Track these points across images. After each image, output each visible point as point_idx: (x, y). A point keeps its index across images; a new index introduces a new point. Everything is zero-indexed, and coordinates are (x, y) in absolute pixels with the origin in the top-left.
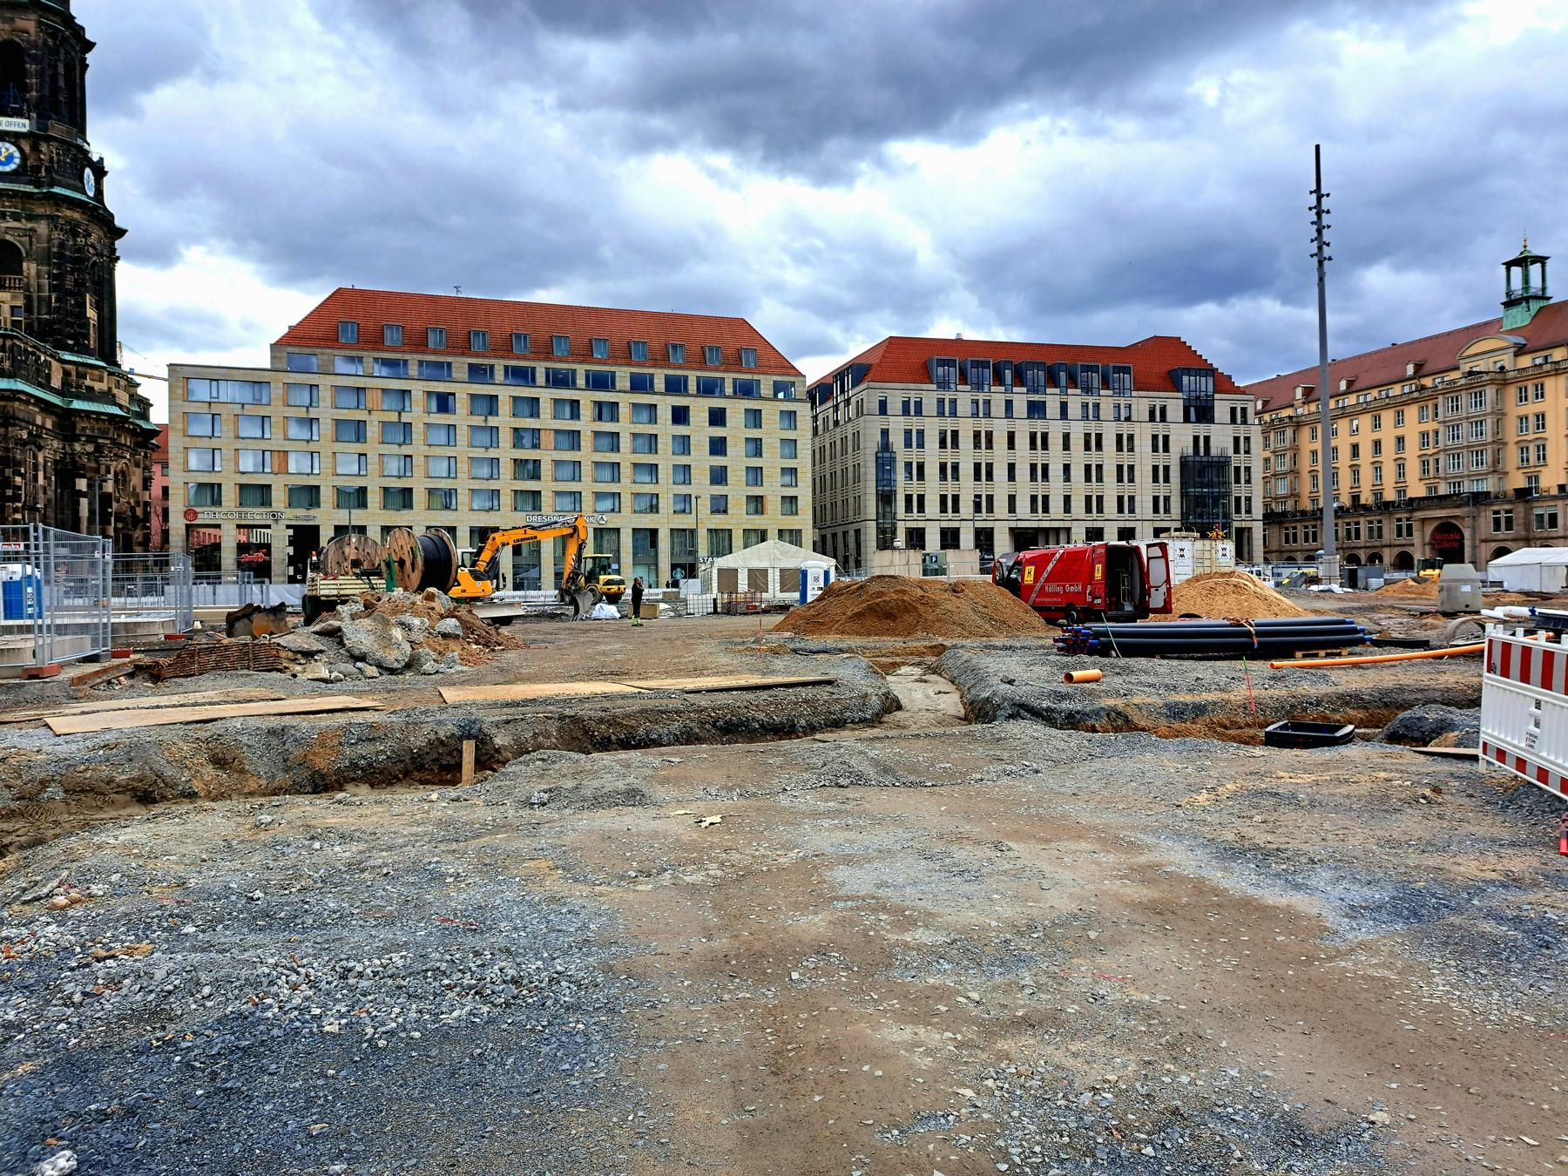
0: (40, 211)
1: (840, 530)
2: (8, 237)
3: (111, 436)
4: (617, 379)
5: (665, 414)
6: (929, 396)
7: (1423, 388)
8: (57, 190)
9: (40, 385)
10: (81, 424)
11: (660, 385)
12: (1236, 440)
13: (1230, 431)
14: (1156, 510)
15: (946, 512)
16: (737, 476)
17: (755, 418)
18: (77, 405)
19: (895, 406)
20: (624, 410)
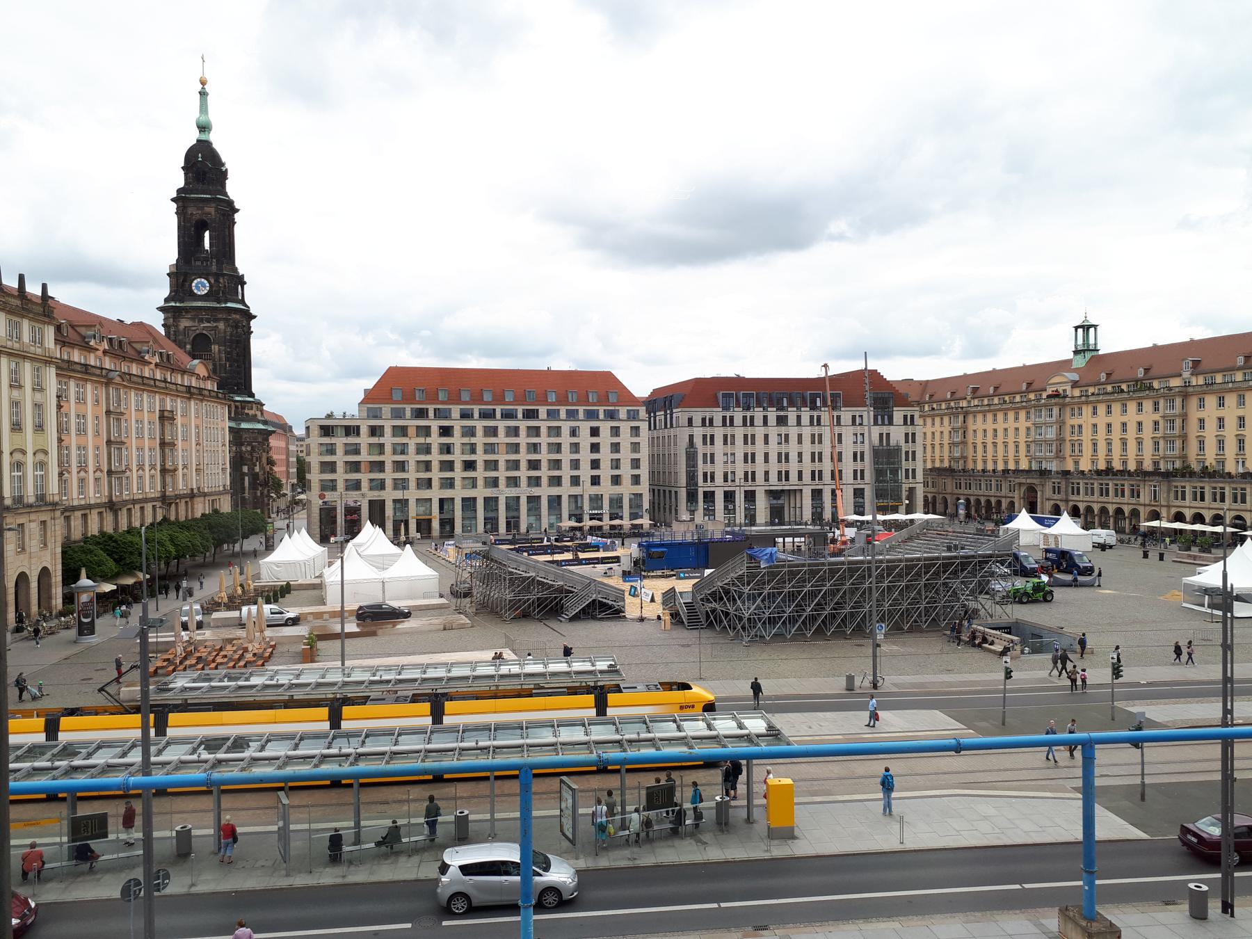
0: (220, 316)
1: (673, 490)
2: (204, 332)
4: (540, 413)
5: (565, 431)
6: (718, 414)
8: (229, 305)
11: (563, 415)
12: (907, 435)
13: (903, 430)
14: (855, 478)
17: (615, 431)
18: (244, 425)
19: (697, 420)
20: (544, 431)
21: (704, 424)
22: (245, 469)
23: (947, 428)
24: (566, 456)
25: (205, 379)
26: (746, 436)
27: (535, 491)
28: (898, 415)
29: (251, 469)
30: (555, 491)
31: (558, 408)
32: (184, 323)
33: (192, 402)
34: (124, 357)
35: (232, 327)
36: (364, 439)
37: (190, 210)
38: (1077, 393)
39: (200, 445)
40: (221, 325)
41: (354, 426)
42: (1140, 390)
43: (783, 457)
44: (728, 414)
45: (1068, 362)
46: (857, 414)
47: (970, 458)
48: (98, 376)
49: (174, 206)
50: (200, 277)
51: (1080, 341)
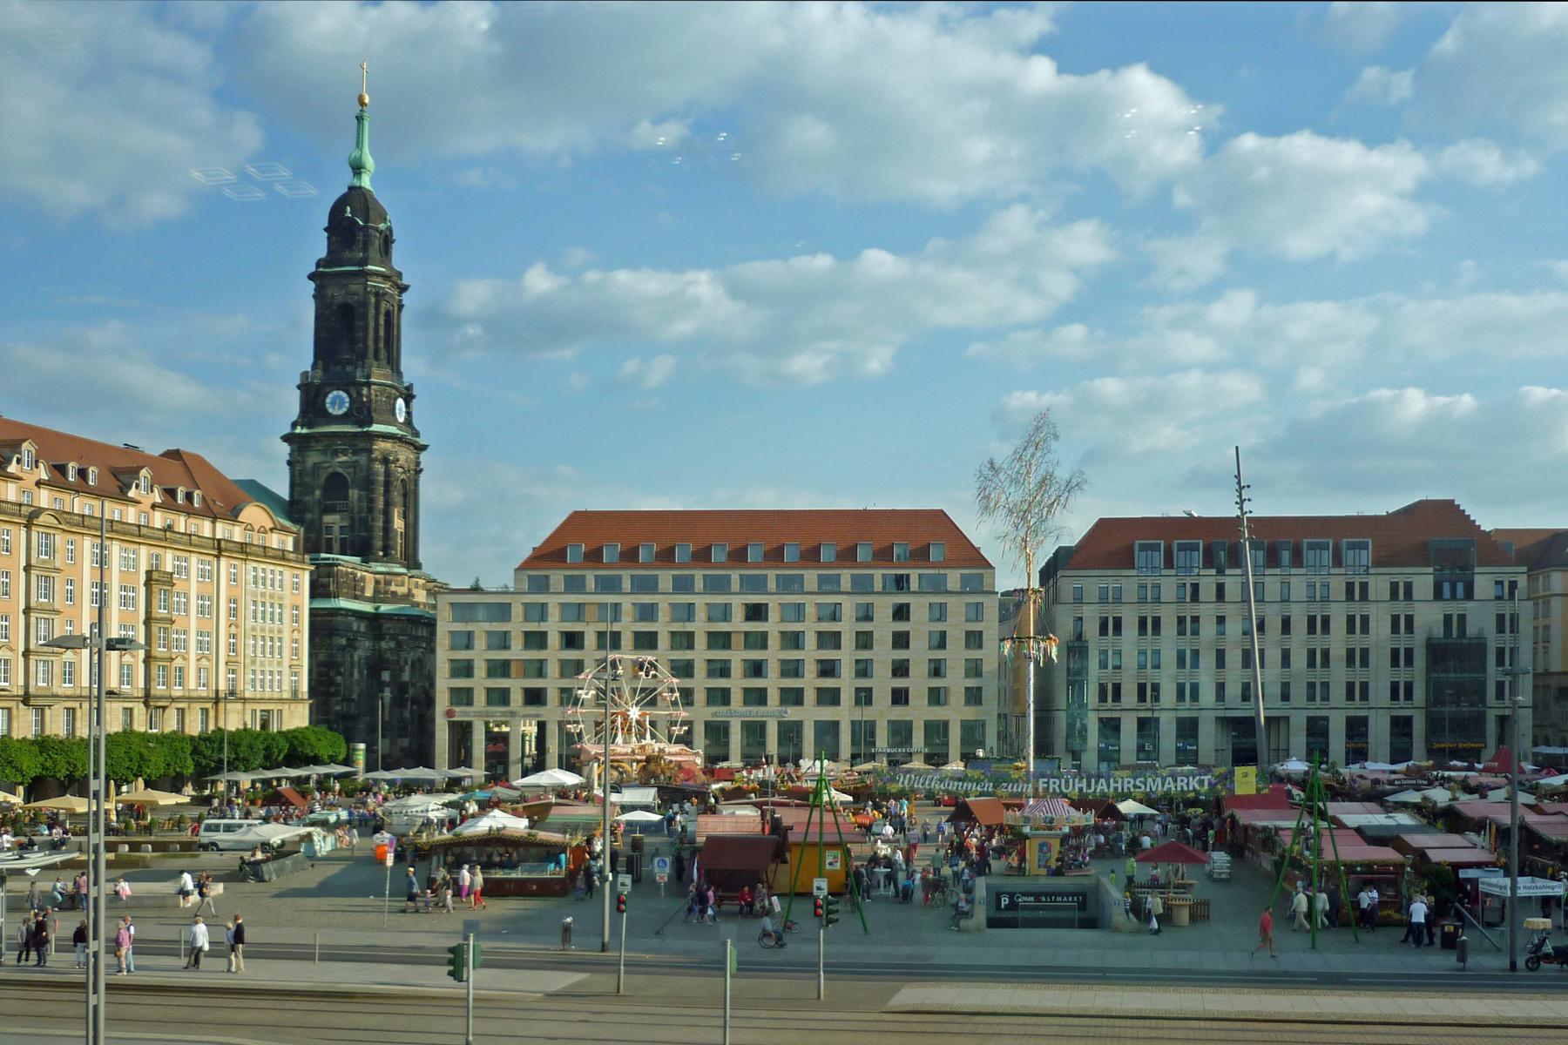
2: (340, 470)
3: (409, 632)
9: (356, 597)
12: (1500, 619)
15: (1106, 701)
16: (919, 669)
17: (940, 613)
24: (846, 656)
27: (792, 714)
30: (827, 713)
32: (313, 458)
37: (330, 291)
46: (1401, 580)
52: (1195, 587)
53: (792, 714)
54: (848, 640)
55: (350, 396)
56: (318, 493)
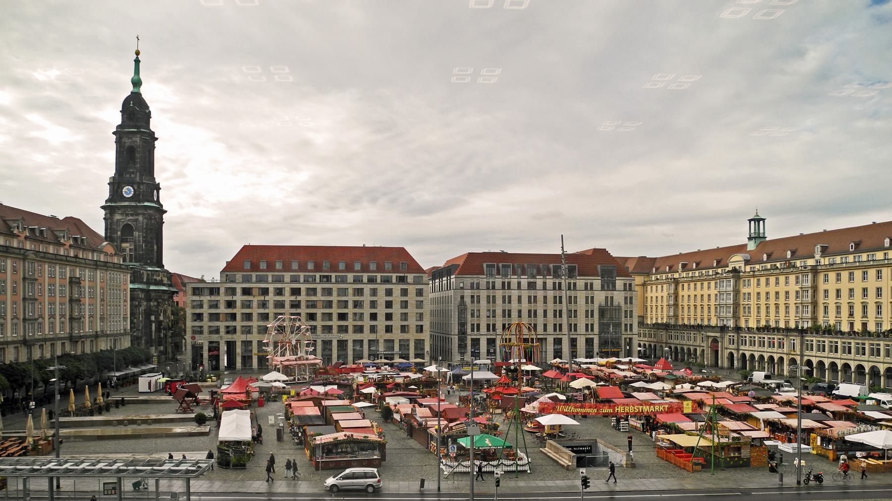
0: (140, 211)
2: (129, 223)
4: (348, 278)
7: (717, 273)
8: (146, 204)
10: (153, 294)
12: (626, 298)
13: (623, 294)
14: (587, 330)
16: (397, 317)
18: (152, 287)
21: (503, 288)
22: (153, 318)
23: (665, 294)
25: (111, 255)
26: (530, 297)
27: (343, 336)
28: (619, 283)
29: (157, 318)
30: (358, 336)
31: (362, 274)
32: (117, 217)
33: (98, 272)
34: (42, 241)
35: (147, 218)
36: (223, 298)
37: (124, 140)
38: (748, 268)
39: (104, 301)
40: (141, 218)
41: (216, 288)
42: (789, 268)
43: (533, 313)
44: (506, 281)
45: (745, 246)
46: (589, 282)
47: (680, 316)
48: (18, 254)
49: (114, 137)
50: (128, 185)
51: (753, 231)
52: (509, 283)
53: (343, 336)
54: (367, 305)
55: (134, 188)
56: (119, 233)
